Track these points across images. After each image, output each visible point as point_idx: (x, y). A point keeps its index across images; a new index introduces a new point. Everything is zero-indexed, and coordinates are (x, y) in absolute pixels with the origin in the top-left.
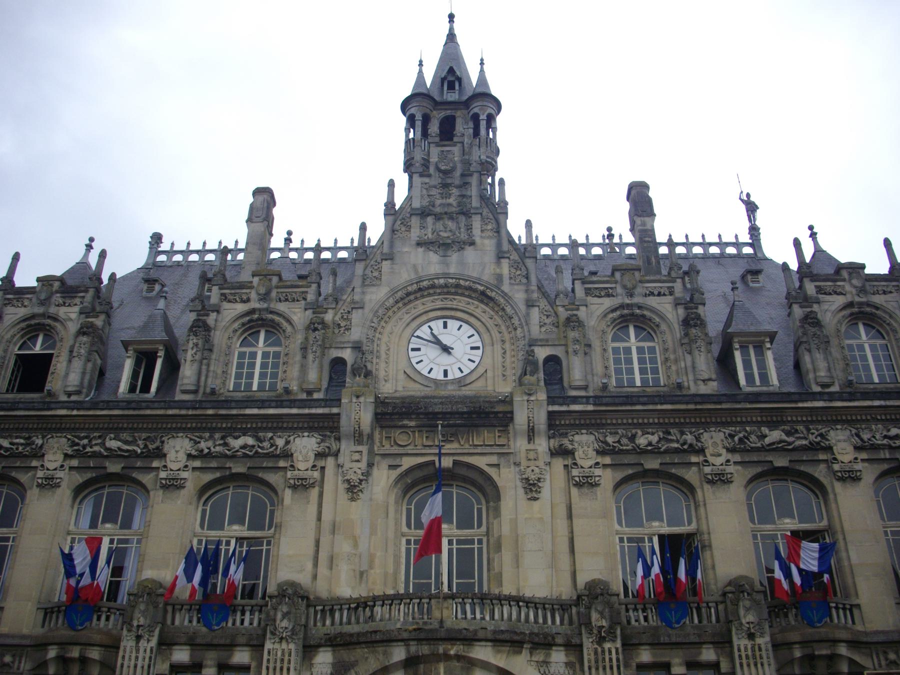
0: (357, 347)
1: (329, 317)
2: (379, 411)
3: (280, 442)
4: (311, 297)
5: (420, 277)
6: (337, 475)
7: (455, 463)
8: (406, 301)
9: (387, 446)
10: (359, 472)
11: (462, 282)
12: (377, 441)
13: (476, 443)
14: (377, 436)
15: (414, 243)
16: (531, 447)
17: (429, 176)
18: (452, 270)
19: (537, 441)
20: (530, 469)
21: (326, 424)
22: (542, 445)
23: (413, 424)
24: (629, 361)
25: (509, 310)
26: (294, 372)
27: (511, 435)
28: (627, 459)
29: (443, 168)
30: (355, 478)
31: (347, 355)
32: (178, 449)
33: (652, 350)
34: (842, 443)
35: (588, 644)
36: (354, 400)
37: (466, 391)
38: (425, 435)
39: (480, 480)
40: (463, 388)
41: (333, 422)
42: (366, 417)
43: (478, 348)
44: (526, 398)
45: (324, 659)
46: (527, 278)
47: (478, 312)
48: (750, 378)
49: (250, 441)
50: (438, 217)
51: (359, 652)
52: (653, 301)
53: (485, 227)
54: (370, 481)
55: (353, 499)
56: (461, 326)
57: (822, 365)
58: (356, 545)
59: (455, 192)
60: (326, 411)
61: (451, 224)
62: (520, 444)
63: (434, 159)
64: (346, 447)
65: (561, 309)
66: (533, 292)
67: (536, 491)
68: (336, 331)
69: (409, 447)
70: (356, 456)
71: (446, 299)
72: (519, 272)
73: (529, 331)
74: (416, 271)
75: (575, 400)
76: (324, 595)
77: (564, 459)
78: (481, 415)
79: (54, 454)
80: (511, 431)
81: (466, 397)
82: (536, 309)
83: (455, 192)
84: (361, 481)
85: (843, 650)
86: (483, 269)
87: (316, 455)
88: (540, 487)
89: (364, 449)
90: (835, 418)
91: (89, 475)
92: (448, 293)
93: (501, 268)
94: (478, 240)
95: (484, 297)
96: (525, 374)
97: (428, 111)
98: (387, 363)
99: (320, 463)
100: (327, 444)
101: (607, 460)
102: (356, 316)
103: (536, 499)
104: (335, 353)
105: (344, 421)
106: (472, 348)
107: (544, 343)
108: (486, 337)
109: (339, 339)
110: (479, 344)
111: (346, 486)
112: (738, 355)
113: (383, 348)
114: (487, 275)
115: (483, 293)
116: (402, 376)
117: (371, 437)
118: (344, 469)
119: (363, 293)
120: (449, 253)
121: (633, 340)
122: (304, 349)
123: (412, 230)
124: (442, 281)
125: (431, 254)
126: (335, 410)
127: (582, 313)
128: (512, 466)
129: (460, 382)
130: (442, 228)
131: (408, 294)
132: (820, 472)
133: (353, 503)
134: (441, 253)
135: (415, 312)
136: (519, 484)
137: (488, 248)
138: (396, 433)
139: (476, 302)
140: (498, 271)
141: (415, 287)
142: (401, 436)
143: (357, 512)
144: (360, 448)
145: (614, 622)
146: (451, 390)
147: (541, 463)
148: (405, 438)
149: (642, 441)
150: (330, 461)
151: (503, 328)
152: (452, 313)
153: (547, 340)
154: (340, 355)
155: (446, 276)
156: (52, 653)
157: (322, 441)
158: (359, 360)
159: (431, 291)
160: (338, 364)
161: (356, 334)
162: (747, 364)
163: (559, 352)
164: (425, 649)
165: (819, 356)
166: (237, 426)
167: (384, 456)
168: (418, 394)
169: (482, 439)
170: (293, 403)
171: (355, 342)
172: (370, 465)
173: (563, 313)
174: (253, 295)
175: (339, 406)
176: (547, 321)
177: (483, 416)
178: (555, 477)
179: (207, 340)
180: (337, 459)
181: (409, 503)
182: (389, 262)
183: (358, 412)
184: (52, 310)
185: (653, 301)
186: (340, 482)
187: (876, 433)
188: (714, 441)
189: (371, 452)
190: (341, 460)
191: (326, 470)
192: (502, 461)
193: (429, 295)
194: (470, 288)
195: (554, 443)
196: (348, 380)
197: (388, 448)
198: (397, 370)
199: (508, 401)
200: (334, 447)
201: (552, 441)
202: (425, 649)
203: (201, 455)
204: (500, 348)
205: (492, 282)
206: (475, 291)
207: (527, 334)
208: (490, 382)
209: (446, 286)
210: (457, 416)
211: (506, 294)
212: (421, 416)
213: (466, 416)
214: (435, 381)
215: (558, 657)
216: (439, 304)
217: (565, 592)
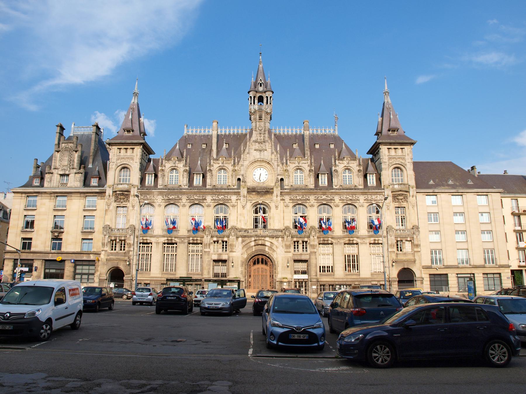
0: (243, 175)
1: (236, 168)
3: (229, 197)
4: (233, 163)
18: (262, 157)
22: (279, 198)
24: (297, 178)
26: (230, 181)
28: (295, 201)
31: (241, 177)
32: (209, 198)
33: (302, 176)
34: (337, 198)
35: (285, 237)
37: (265, 185)
42: (246, 193)
45: (240, 239)
48: (322, 182)
49: (223, 197)
50: (259, 143)
51: (246, 238)
52: (303, 165)
57: (336, 181)
58: (244, 218)
59: (262, 135)
62: (274, 198)
63: (258, 126)
64: (242, 198)
75: (286, 189)
76: (239, 227)
78: (268, 191)
79: (184, 199)
83: (262, 135)
85: (330, 239)
90: (337, 194)
91: (192, 204)
101: (291, 201)
104: (238, 177)
107: (280, 175)
112: (320, 177)
114: (269, 159)
121: (299, 174)
122: (232, 176)
127: (288, 168)
129: (263, 183)
132: (332, 205)
138: (251, 195)
143: (245, 211)
145: (290, 233)
146: (261, 185)
149: (298, 198)
156: (191, 239)
160: (239, 179)
161: (242, 172)
162: (322, 179)
163: (283, 177)
164: (258, 238)
165: (336, 179)
166: (220, 194)
170: (231, 189)
173: (285, 168)
174: (220, 163)
178: (281, 205)
179: (212, 173)
183: (244, 191)
184: (176, 165)
185: (303, 165)
187: (344, 197)
188: (312, 198)
195: (281, 198)
199: (272, 189)
202: (258, 238)
203: (214, 200)
215: (280, 239)
217: (282, 227)
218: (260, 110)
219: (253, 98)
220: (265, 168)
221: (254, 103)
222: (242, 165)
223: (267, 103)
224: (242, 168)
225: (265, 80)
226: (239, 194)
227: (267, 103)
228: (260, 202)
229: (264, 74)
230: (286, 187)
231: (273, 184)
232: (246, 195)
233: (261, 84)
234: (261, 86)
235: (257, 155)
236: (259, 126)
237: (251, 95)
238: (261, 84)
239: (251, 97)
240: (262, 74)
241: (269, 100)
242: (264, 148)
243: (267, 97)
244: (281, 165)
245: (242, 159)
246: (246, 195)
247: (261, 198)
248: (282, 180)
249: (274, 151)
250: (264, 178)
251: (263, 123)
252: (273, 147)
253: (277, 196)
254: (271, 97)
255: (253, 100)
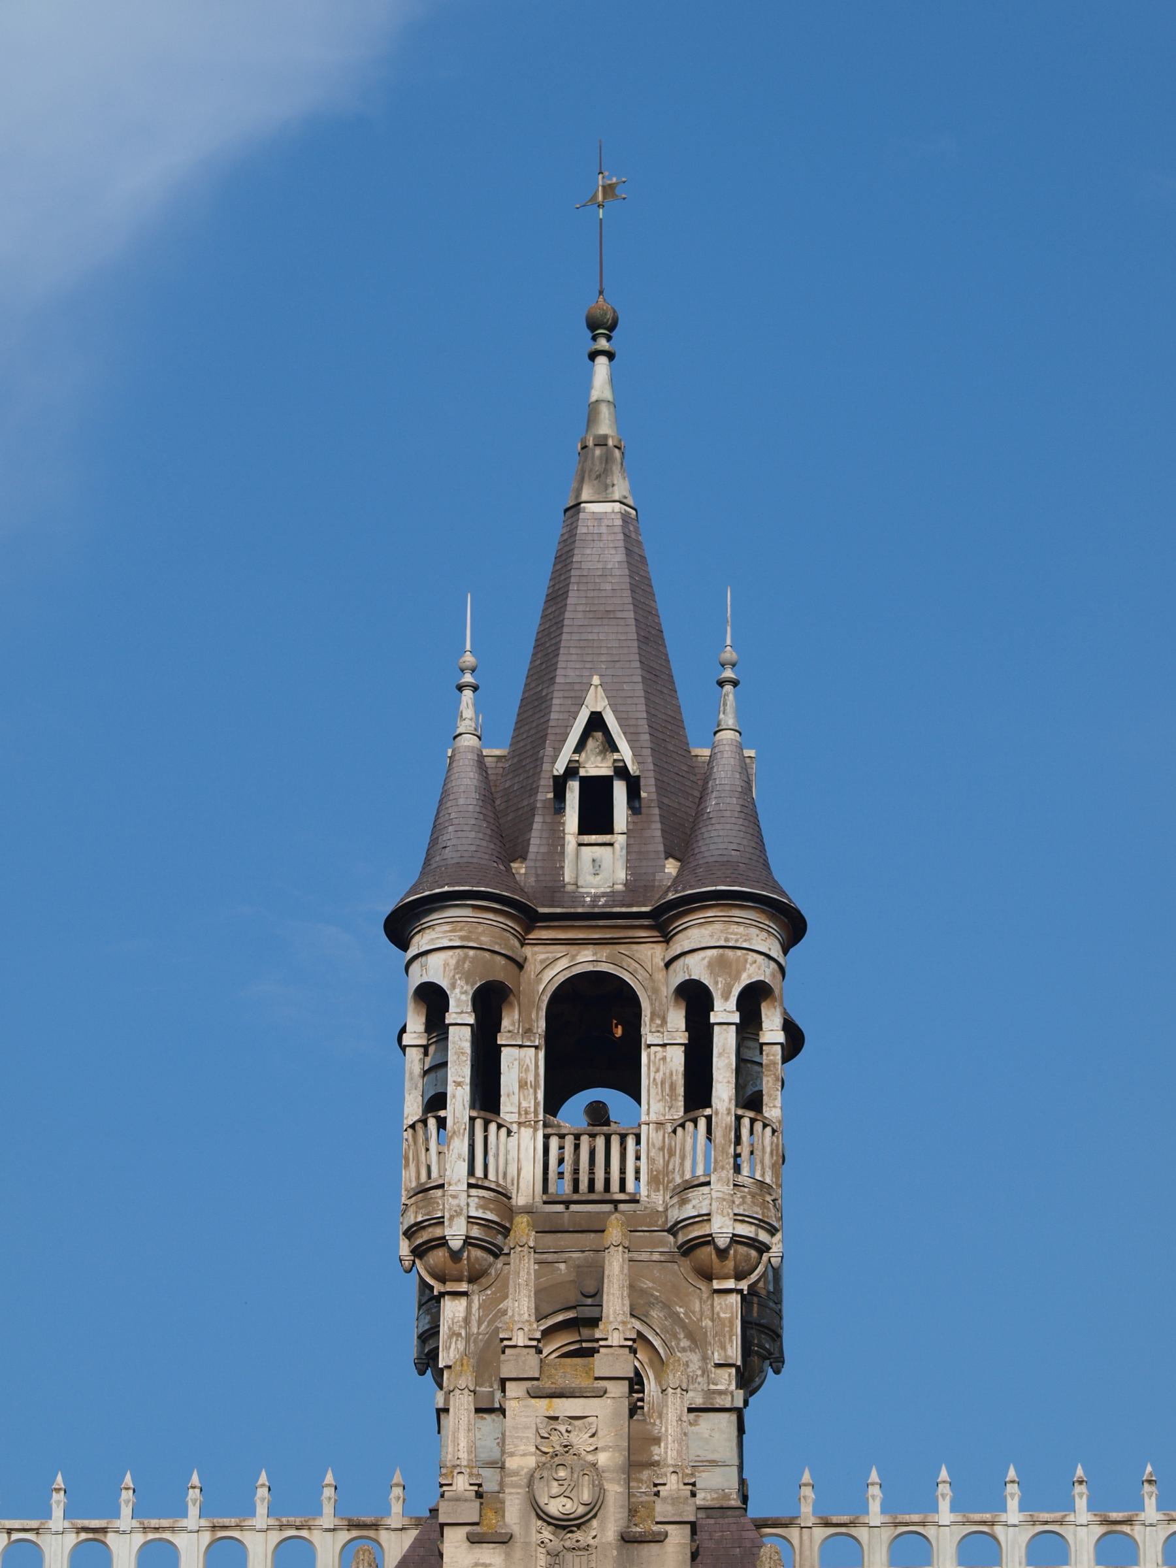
17: (504, 1540)
29: (555, 1508)
97: (500, 971)
218: (582, 1206)
219: (460, 1011)
221: (486, 1095)
223: (697, 1089)
225: (666, 731)
227: (697, 1089)
229: (650, 637)
233: (596, 800)
234: (596, 819)
236: (557, 1457)
237: (436, 970)
238: (596, 800)
239: (433, 999)
240: (621, 636)
241: (724, 1043)
243: (695, 998)
251: (605, 1412)
254: (753, 999)
255: (460, 1041)
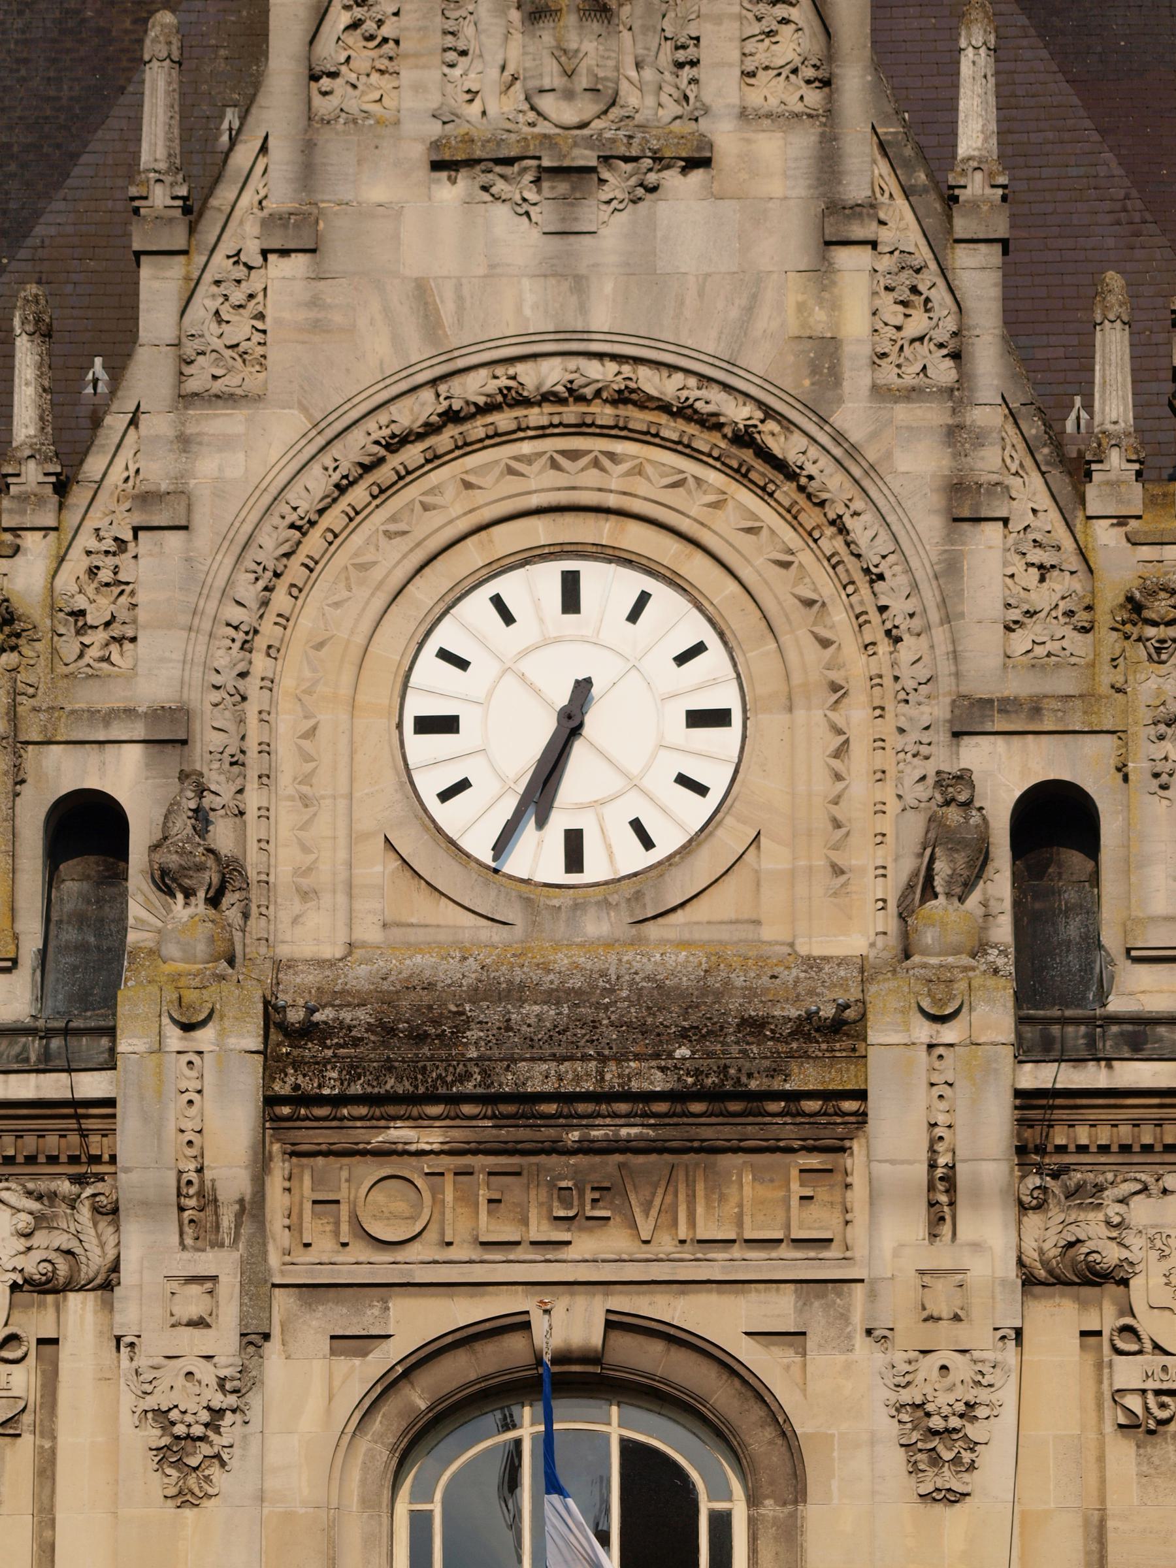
0: (169, 736)
2: (281, 1088)
5: (450, 354)
6: (106, 1379)
7: (615, 1324)
8: (384, 475)
9: (324, 1247)
10: (207, 1373)
11: (649, 382)
12: (276, 1220)
13: (702, 1234)
14: (277, 1200)
15: (418, 153)
16: (942, 1256)
18: (603, 316)
19: (969, 1225)
20: (935, 1360)
21: (52, 1143)
22: (991, 1241)
23: (431, 1139)
25: (861, 529)
27: (858, 1196)
30: (191, 1404)
31: (125, 776)
36: (174, 1038)
37: (670, 953)
38: (483, 1194)
39: (720, 1395)
40: (653, 931)
41: (83, 1134)
42: (230, 1125)
43: (720, 718)
44: (923, 1031)
46: (956, 356)
47: (722, 530)
53: (762, 53)
54: (254, 1415)
55: (184, 1498)
56: (644, 599)
60: (51, 1086)
61: (588, 44)
64: (147, 1251)
65: (1106, 536)
66: (979, 439)
67: (956, 1461)
68: (69, 647)
69: (414, 1252)
70: (193, 1303)
71: (573, 455)
72: (917, 323)
73: (955, 655)
74: (431, 324)
77: (1083, 1304)
80: (858, 1179)
81: (660, 993)
82: (993, 531)
84: (218, 1413)
86: (750, 310)
87: (15, 1287)
88: (972, 1446)
89: (223, 1263)
92: (582, 428)
93: (834, 306)
94: (725, 136)
95: (750, 455)
96: (929, 891)
98: (305, 801)
99: (36, 1322)
100: (62, 1240)
102: (154, 567)
103: (954, 1498)
104: (65, 772)
105: (130, 1139)
106: (699, 719)
107: (1021, 717)
108: (760, 658)
109: (89, 696)
110: (726, 697)
111: (154, 1435)
113: (286, 723)
114: (767, 359)
115: (744, 438)
116: (377, 868)
117: (252, 1209)
118: (142, 1361)
119: (184, 442)
120: (591, 213)
123: (408, 75)
124: (551, 374)
125: (502, 212)
126: (91, 1085)
128: (859, 1338)
129: (642, 898)
130: (551, 76)
131: (397, 442)
133: (188, 1512)
134: (545, 215)
135: (435, 528)
136: (888, 1428)
137: (776, 187)
138: (355, 1181)
139: (714, 478)
140: (819, 318)
141: (425, 406)
142: (379, 1196)
144: (207, 1262)
147: (978, 1334)
148: (401, 1207)
150: (80, 1308)
151: (840, 617)
152: (603, 531)
153: (1035, 709)
154: (92, 782)
155: (573, 345)
157: (41, 1221)
158: (182, 826)
159: (504, 420)
160: (87, 828)
161: (157, 670)
163: (1082, 764)
167: (313, 1291)
168: (449, 971)
169: (731, 1209)
171: (159, 714)
172: (255, 1339)
175: (110, 1064)
176: (1044, 596)
177: (734, 1107)
180: (108, 1307)
181: (423, 1492)
182: (299, 262)
183: (188, 1096)
186: (127, 1420)
189: (258, 1286)
190: (131, 1312)
191: (65, 1351)
192: (818, 1325)
193: (497, 438)
194: (684, 412)
195: (1043, 1235)
196: (135, 910)
197: (328, 1255)
198: (354, 839)
199: (842, 1030)
200: (94, 1261)
201: (1033, 1221)
204: (822, 731)
205: (787, 384)
206: (710, 422)
207: (945, 668)
208: (773, 900)
209: (574, 394)
210: (623, 1107)
211: (854, 451)
212: (467, 1109)
213: (662, 1107)
214: (528, 890)
216: (542, 485)
220: (669, 556)
222: (161, 511)
224: (154, 567)
226: (90, 1166)
228: (572, 1326)
230: (1141, 991)
231: (854, 932)
232: (230, 1174)
235: (474, 271)
242: (649, 103)
244: (1031, 495)
245: (150, 376)
246: (230, 1174)
247: (596, 1249)
248: (1057, 821)
249: (865, 172)
250: (639, 787)
252: (854, 80)
253: (943, 1192)
